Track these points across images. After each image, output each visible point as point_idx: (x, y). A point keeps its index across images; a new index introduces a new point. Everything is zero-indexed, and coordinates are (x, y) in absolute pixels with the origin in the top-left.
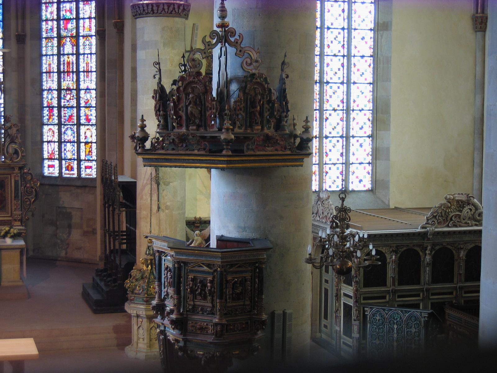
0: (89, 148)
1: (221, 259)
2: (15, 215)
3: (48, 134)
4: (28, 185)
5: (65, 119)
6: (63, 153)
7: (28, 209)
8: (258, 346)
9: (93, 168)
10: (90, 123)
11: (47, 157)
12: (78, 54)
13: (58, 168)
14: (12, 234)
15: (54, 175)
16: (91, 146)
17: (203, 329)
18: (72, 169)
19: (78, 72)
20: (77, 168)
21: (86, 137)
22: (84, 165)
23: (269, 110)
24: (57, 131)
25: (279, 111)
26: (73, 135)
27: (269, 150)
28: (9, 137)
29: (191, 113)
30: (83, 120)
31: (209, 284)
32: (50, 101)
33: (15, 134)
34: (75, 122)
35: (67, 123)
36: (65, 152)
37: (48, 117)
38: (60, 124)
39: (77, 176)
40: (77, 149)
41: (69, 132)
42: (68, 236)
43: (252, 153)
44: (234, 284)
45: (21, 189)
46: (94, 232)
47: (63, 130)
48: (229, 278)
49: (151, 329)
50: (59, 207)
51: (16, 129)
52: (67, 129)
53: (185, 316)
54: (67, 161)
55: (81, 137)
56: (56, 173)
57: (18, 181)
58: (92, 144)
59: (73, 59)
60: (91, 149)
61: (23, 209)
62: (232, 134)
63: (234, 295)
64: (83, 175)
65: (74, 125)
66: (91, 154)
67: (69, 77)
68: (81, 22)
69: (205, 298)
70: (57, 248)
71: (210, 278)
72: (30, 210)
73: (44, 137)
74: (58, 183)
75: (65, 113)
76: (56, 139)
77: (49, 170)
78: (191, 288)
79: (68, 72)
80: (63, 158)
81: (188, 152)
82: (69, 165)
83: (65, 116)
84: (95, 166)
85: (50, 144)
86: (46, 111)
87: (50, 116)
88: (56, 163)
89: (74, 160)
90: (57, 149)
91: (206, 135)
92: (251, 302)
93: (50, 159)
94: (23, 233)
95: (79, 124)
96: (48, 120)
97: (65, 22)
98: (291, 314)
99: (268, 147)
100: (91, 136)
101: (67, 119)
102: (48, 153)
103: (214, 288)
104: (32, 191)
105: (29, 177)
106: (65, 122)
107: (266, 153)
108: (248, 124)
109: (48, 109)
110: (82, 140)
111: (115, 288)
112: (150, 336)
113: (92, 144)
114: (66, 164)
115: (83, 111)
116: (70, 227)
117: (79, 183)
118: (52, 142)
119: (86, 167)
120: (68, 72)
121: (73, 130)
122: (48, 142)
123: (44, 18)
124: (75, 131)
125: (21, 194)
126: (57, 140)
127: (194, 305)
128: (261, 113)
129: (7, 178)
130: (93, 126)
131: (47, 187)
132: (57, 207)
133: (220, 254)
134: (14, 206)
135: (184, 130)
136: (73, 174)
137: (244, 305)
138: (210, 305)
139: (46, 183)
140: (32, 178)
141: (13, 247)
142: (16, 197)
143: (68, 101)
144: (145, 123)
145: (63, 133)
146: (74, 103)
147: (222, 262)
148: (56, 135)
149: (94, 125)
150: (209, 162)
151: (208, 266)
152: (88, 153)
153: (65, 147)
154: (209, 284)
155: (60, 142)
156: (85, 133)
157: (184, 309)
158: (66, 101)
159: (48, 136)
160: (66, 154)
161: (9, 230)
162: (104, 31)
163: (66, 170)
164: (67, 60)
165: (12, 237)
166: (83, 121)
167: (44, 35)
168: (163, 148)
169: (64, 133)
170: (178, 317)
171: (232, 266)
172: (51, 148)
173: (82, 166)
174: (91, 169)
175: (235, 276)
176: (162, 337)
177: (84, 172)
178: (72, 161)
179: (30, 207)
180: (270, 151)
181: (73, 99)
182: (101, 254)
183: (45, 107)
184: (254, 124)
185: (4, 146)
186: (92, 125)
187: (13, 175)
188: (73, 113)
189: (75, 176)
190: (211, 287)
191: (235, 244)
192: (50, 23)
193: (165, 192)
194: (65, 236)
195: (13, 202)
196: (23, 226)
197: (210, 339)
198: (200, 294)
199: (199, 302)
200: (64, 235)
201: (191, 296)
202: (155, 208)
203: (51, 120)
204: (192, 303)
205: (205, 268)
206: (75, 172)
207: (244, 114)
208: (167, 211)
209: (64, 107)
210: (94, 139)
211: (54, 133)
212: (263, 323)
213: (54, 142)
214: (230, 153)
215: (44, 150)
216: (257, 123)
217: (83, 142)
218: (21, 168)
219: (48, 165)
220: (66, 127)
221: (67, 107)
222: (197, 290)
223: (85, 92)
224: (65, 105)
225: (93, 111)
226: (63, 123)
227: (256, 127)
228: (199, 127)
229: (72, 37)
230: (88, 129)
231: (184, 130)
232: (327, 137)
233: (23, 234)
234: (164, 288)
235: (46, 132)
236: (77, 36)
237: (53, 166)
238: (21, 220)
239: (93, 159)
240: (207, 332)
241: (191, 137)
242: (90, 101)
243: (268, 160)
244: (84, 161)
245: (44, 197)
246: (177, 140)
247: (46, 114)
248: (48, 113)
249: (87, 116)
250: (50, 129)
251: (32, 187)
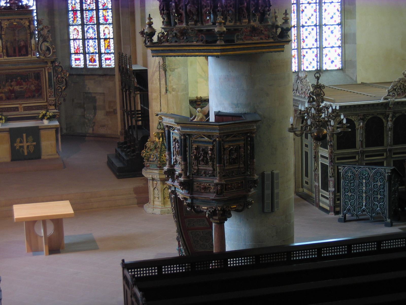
0: (108, 44)
1: (219, 131)
2: (50, 101)
3: (74, 34)
4: (59, 76)
5: (87, 20)
6: (86, 49)
7: (61, 95)
8: (252, 201)
9: (112, 60)
10: (108, 23)
11: (74, 52)
13: (83, 61)
14: (48, 116)
15: (80, 67)
16: (109, 41)
17: (206, 189)
18: (95, 61)
20: (99, 60)
21: (105, 34)
22: (104, 57)
23: (254, 6)
24: (81, 30)
25: (262, 6)
26: (94, 33)
27: (256, 39)
28: (42, 37)
29: (190, 11)
30: (102, 20)
31: (209, 152)
32: (74, 6)
33: (46, 34)
34: (96, 23)
35: (89, 23)
36: (88, 47)
37: (73, 19)
38: (83, 25)
39: (99, 66)
40: (98, 44)
41: (91, 31)
42: (94, 116)
43: (241, 42)
44: (230, 151)
45: (54, 79)
46: (115, 112)
47: (86, 29)
48: (226, 146)
49: (164, 189)
50: (85, 93)
51: (47, 30)
52: (89, 28)
53: (191, 178)
54: (90, 54)
55: (101, 35)
56: (82, 65)
57: (51, 72)
58: (109, 39)
60: (109, 44)
61: (56, 96)
62: (225, 27)
63: (231, 160)
64: (104, 66)
66: (110, 48)
69: (207, 163)
70: (86, 126)
71: (210, 147)
72: (62, 96)
73: (71, 36)
74: (84, 73)
75: (87, 15)
76: (80, 36)
77: (76, 63)
78: (195, 156)
80: (87, 52)
81: (188, 44)
82: (92, 58)
83: (87, 18)
84: (114, 58)
85: (76, 41)
86: (71, 14)
87: (75, 18)
88: (81, 57)
89: (96, 53)
90: (81, 45)
91: (202, 29)
92: (245, 165)
93: (76, 53)
94: (57, 115)
95: (98, 24)
96: (73, 21)
98: (277, 174)
99: (255, 36)
100: (109, 33)
101: (89, 20)
102: (74, 49)
103: (214, 155)
104: (63, 80)
105: (60, 69)
106: (87, 23)
107: (253, 42)
108: (237, 18)
109: (72, 12)
110: (101, 37)
111: (133, 157)
112: (164, 195)
113: (109, 39)
114: (89, 57)
115: (101, 12)
116: (95, 108)
117: (101, 72)
118: (77, 39)
119: (106, 59)
121: (94, 29)
122: (74, 40)
124: (96, 29)
125: (54, 82)
126: (81, 38)
127: (198, 169)
128: (248, 9)
129: (42, 71)
130: (110, 25)
131: (75, 76)
132: (84, 93)
133: (218, 126)
134: (49, 93)
135: (184, 25)
136: (96, 65)
137: (239, 168)
138: (211, 169)
139: (73, 73)
140: (62, 70)
141: (49, 127)
142: (50, 86)
143: (88, 5)
144: (152, 20)
145: (86, 32)
146: (93, 6)
147: (220, 133)
148: (80, 33)
149: (111, 24)
150: (206, 51)
151: (209, 137)
152: (107, 47)
153: (88, 43)
154: (209, 152)
155: (84, 39)
156: (104, 31)
157: (190, 173)
158: (87, 5)
159: (73, 35)
160: (89, 49)
161: (46, 113)
163: (90, 62)
165: (48, 119)
166: (101, 21)
168: (167, 41)
169: (87, 31)
170: (186, 179)
171: (228, 136)
172: (77, 45)
173: (102, 58)
174: (110, 61)
175: (231, 144)
176: (173, 196)
177: (104, 63)
178: (94, 54)
179: (62, 94)
180: (256, 40)
181: (92, 3)
182: (121, 130)
183: (70, 11)
184: (242, 18)
185: (38, 45)
186: (109, 24)
187: (46, 69)
188: (93, 15)
189: (98, 66)
190: (212, 154)
191: (230, 118)
193: (171, 77)
194: (92, 116)
195: (48, 90)
196: (57, 110)
197: (212, 196)
198: (203, 160)
199: (202, 167)
200: (90, 115)
201: (195, 162)
202: (163, 91)
203: (75, 21)
204: (196, 168)
205: (206, 139)
206: (97, 63)
207: (233, 10)
208: (173, 93)
209: (86, 10)
210: (111, 36)
211: (78, 32)
212: (255, 182)
213: (79, 39)
214: (223, 43)
215: (71, 46)
216: (245, 17)
217: (102, 39)
218: (53, 62)
219: (75, 58)
220: (88, 27)
221: (88, 10)
222: (200, 157)
224: (86, 8)
225: (109, 12)
226: (85, 23)
227: (244, 21)
228: (196, 22)
230: (106, 28)
231: (184, 25)
232: (303, 26)
233: (57, 116)
234: (174, 156)
235: (72, 31)
237: (79, 59)
238: (55, 105)
239: (111, 52)
240: (210, 191)
241: (190, 31)
242: (107, 4)
243: (255, 47)
244: (104, 54)
245: (72, 85)
246: (178, 34)
247: (71, 17)
248: (73, 15)
249: (104, 16)
250: (75, 29)
251: (63, 78)
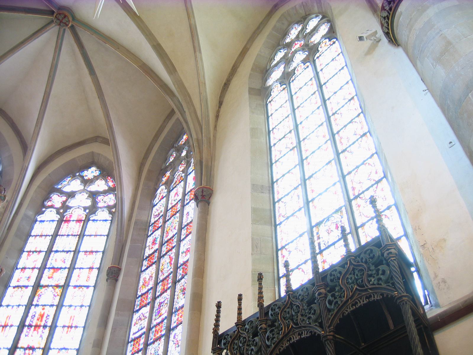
12: (59, 306)
19: (53, 328)
59: (51, 311)
67: (36, 332)
68: (76, 272)
79: (37, 327)
97: (52, 271)
120: (37, 327)
123: (20, 266)
162: (120, 270)
164: (41, 312)
167: (13, 283)
192: (28, 272)
223: (59, 352)
229: (57, 286)
236: (65, 287)
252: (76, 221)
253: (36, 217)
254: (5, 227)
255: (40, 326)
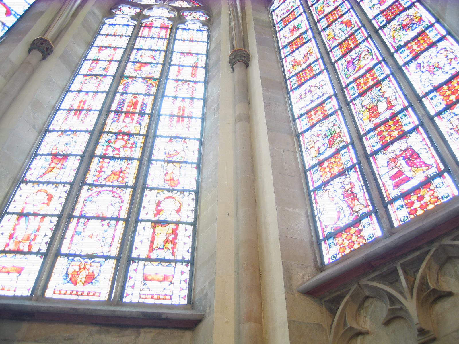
16: (175, 232)
65: (126, 187)
83: (100, 172)
149: (189, 192)
186: (182, 191)
223: (170, 141)
244: (142, 263)
252: (160, 27)
253: (104, 19)
254: (69, 13)
255: (134, 113)
